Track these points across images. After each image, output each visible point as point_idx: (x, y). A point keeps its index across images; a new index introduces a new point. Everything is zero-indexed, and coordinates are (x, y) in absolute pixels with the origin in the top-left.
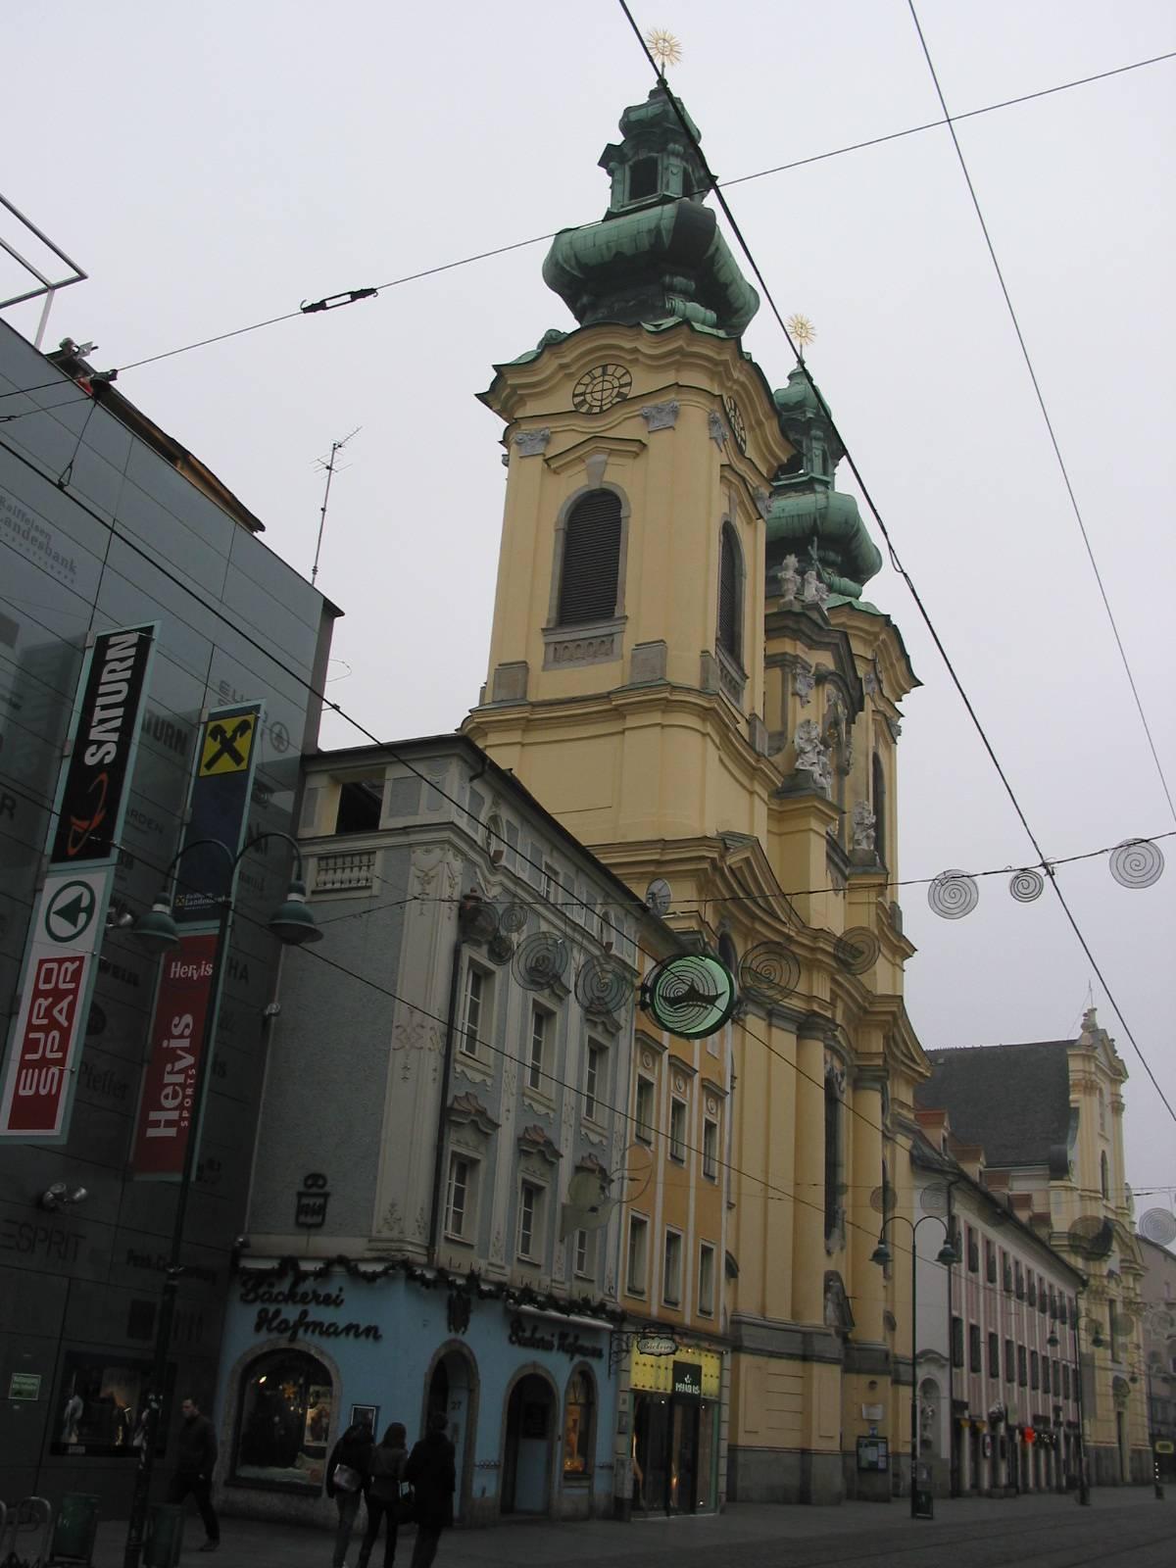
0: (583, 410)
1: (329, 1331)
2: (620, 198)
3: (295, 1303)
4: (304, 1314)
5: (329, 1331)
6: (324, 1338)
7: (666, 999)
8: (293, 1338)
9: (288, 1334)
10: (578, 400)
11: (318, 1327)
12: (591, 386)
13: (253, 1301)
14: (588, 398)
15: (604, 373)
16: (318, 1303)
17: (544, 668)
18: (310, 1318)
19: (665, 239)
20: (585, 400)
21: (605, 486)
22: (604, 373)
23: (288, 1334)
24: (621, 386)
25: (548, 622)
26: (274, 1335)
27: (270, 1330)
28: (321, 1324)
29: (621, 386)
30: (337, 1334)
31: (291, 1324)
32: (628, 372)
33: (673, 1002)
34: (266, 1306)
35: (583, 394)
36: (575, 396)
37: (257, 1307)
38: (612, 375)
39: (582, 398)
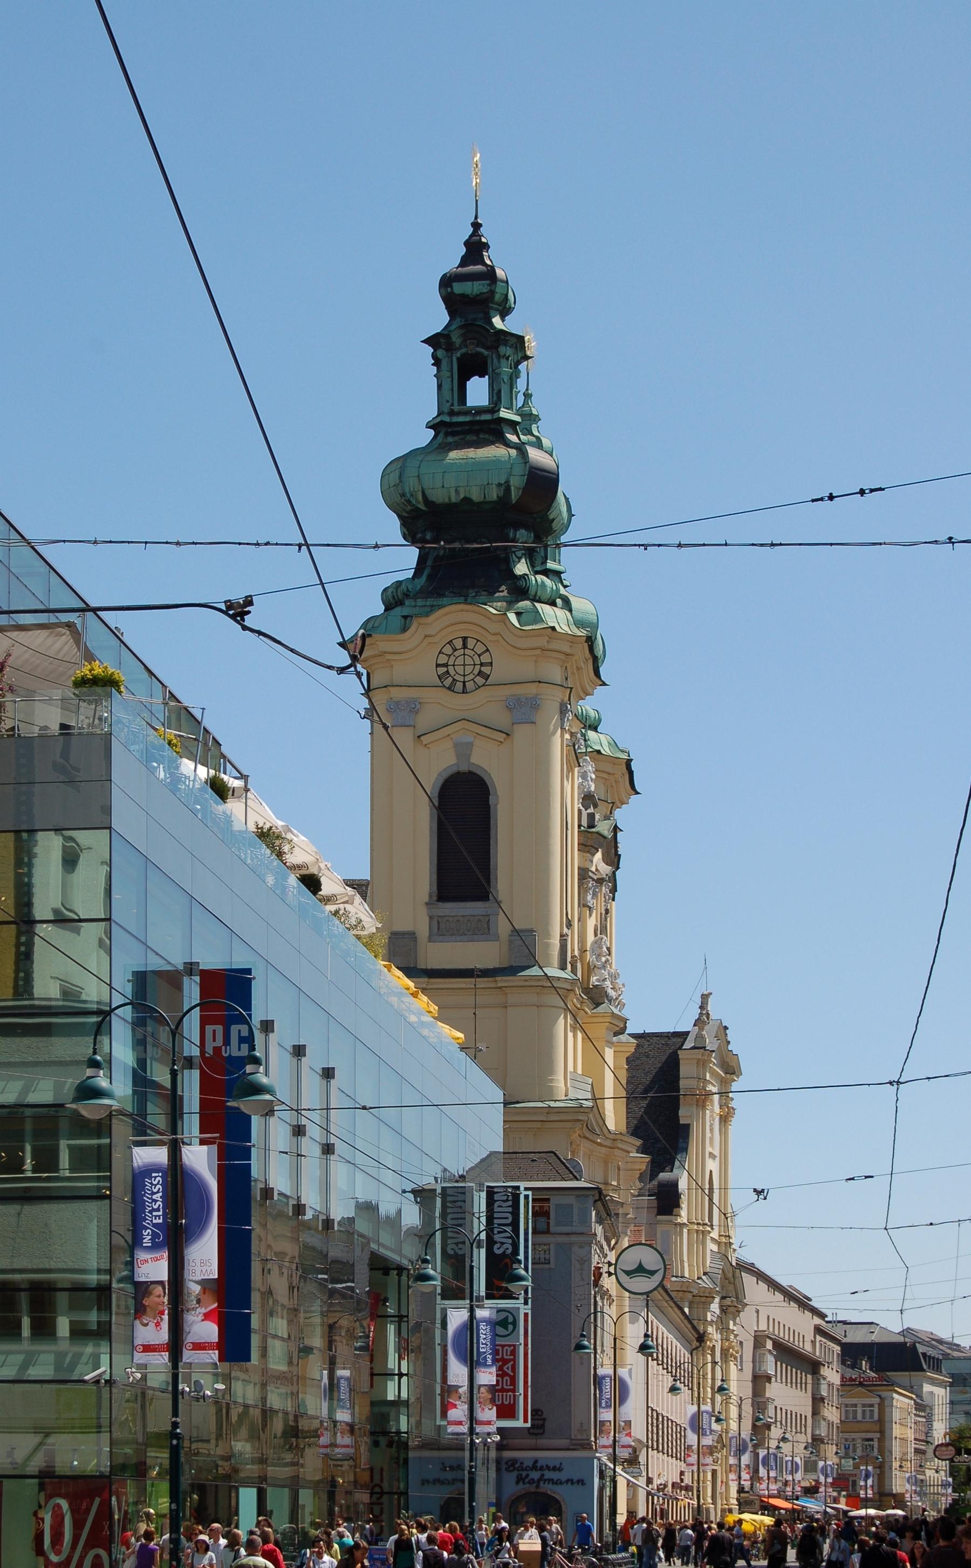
0: (448, 682)
1: (558, 1482)
2: (448, 397)
3: (536, 1470)
4: (543, 1475)
5: (558, 1482)
6: (555, 1485)
7: (624, 1271)
8: (538, 1487)
9: (535, 1485)
10: (442, 670)
11: (551, 1481)
12: (452, 658)
13: (514, 1470)
14: (451, 669)
15: (465, 646)
16: (549, 1470)
17: (430, 939)
18: (546, 1477)
19: (513, 497)
20: (447, 672)
21: (471, 769)
22: (465, 646)
23: (535, 1485)
24: (482, 664)
25: (430, 896)
26: (527, 1485)
27: (524, 1483)
28: (553, 1480)
29: (482, 664)
30: (561, 1483)
31: (536, 1480)
32: (488, 650)
33: (628, 1273)
34: (521, 1472)
35: (446, 665)
36: (438, 665)
37: (515, 1473)
38: (473, 650)
39: (445, 669)
